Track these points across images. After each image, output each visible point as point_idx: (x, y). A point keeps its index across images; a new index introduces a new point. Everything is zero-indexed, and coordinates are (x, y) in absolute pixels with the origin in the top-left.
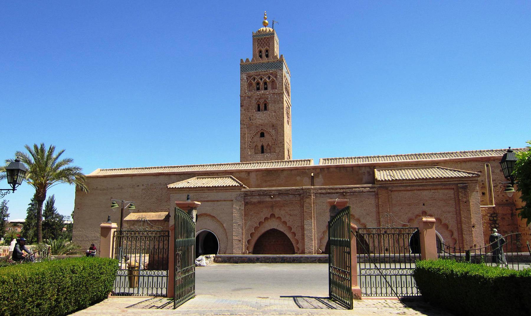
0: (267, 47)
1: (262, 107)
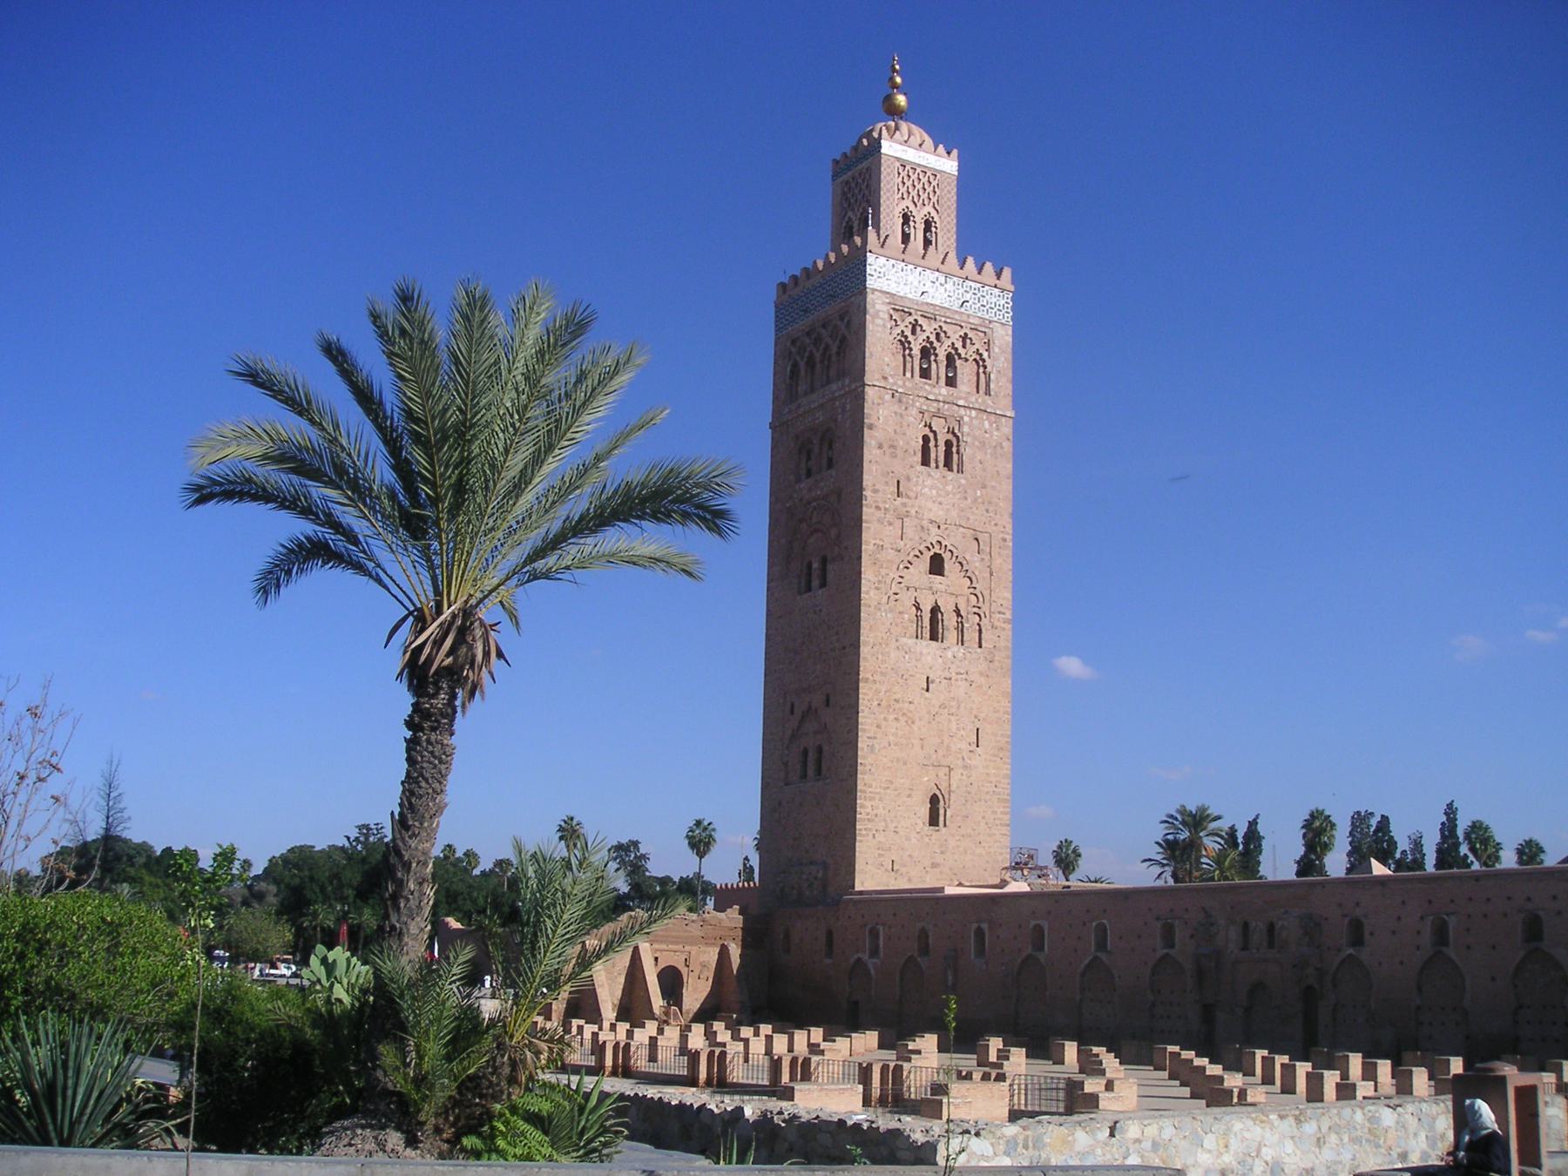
1: (938, 453)
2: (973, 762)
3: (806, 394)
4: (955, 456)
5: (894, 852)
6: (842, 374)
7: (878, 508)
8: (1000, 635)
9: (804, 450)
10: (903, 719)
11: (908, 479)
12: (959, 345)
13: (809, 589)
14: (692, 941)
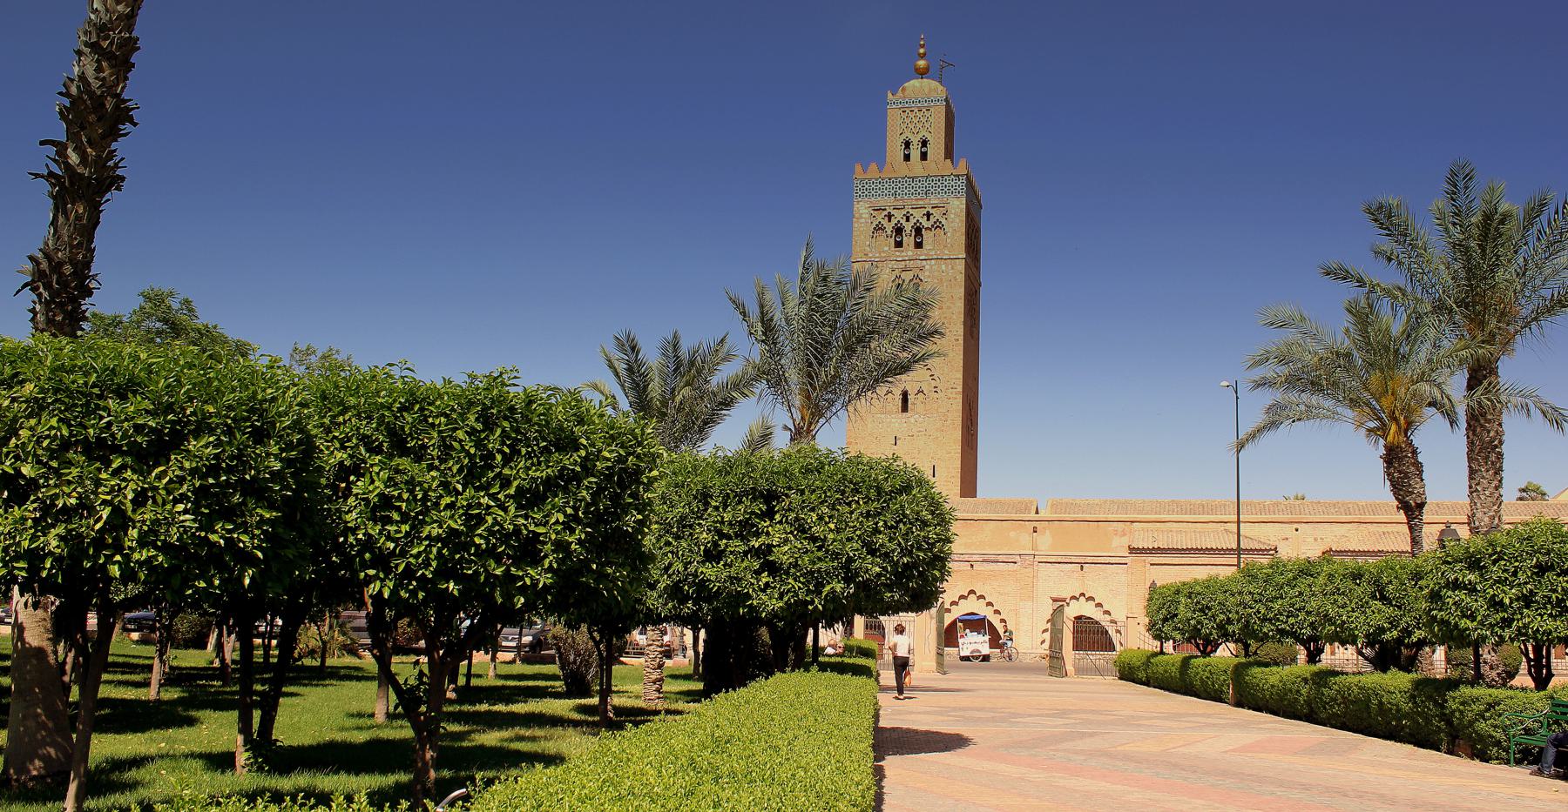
0: (923, 133)
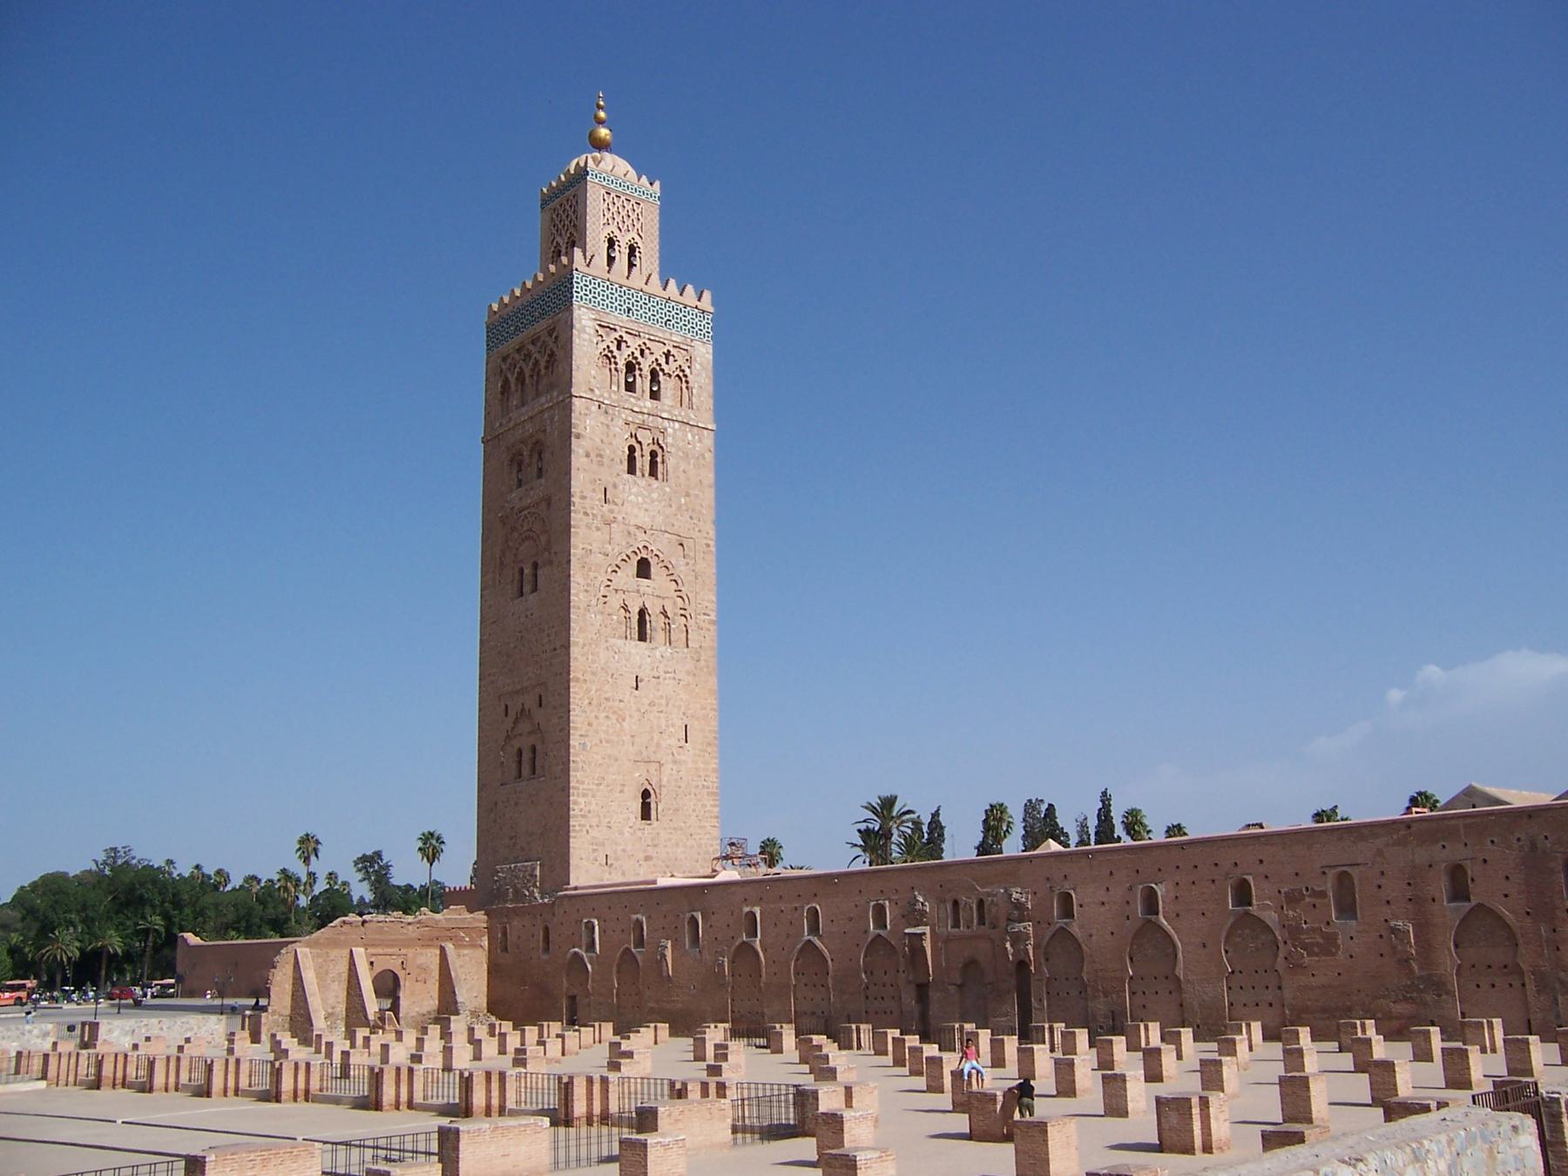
1: (643, 463)
2: (683, 757)
3: (517, 407)
4: (660, 466)
5: (606, 848)
6: (552, 387)
7: (586, 514)
8: (705, 636)
9: (517, 462)
10: (614, 717)
11: (615, 486)
12: (662, 360)
13: (522, 594)
14: (408, 943)
